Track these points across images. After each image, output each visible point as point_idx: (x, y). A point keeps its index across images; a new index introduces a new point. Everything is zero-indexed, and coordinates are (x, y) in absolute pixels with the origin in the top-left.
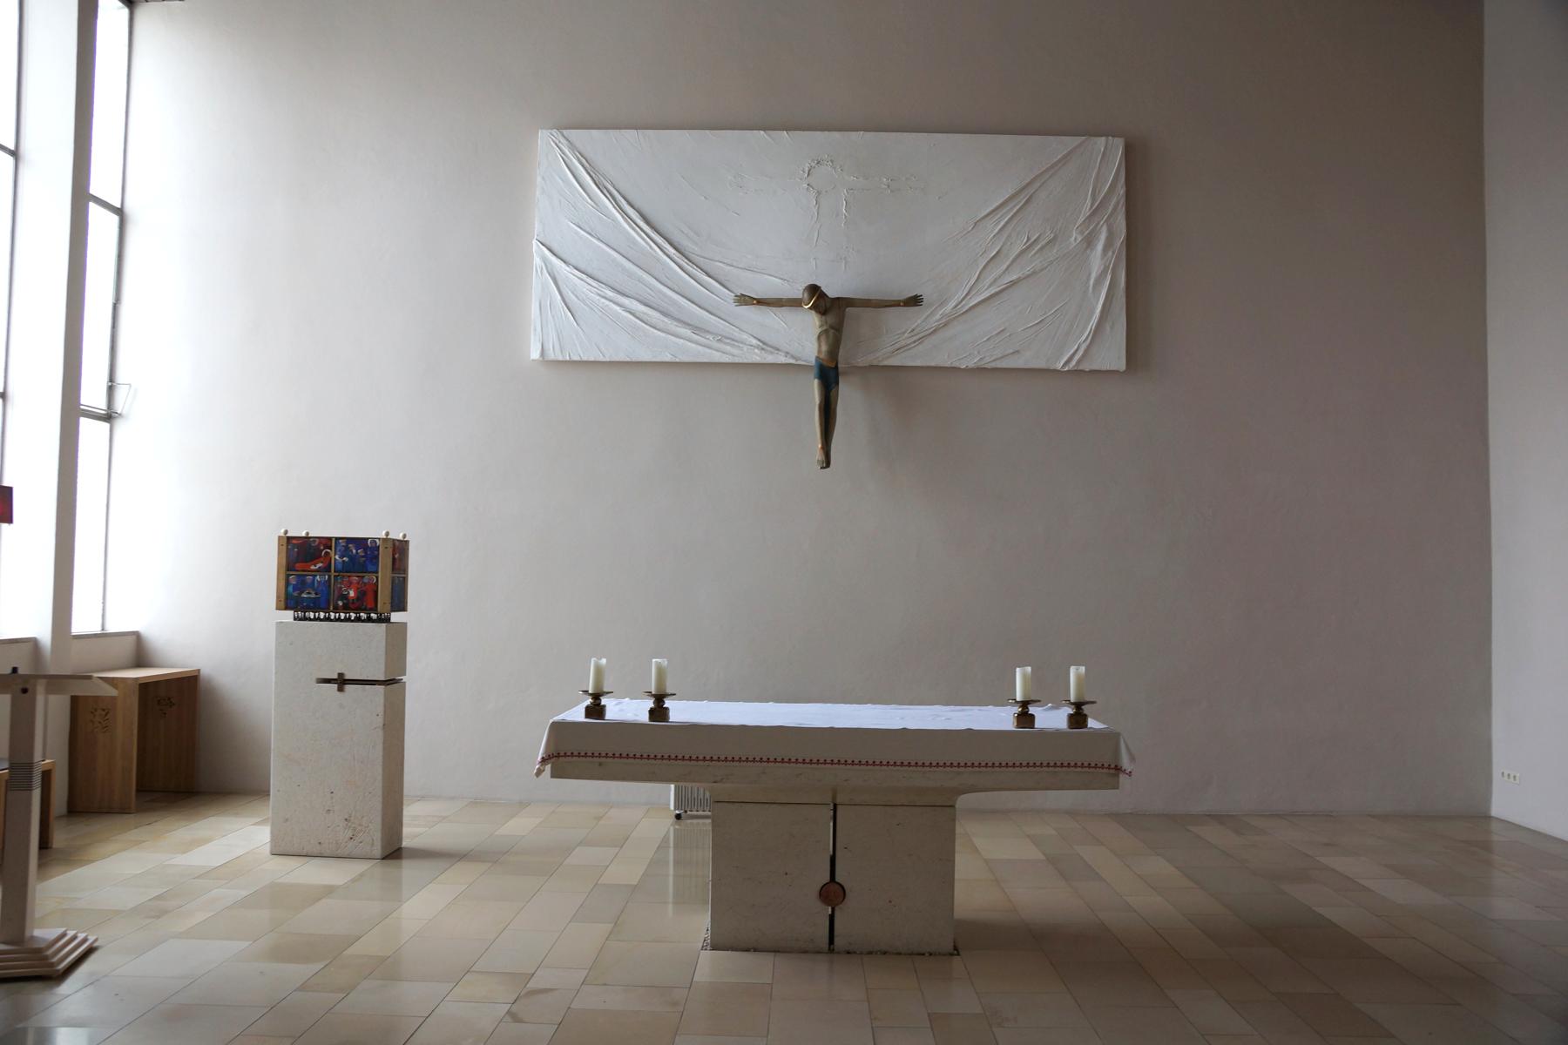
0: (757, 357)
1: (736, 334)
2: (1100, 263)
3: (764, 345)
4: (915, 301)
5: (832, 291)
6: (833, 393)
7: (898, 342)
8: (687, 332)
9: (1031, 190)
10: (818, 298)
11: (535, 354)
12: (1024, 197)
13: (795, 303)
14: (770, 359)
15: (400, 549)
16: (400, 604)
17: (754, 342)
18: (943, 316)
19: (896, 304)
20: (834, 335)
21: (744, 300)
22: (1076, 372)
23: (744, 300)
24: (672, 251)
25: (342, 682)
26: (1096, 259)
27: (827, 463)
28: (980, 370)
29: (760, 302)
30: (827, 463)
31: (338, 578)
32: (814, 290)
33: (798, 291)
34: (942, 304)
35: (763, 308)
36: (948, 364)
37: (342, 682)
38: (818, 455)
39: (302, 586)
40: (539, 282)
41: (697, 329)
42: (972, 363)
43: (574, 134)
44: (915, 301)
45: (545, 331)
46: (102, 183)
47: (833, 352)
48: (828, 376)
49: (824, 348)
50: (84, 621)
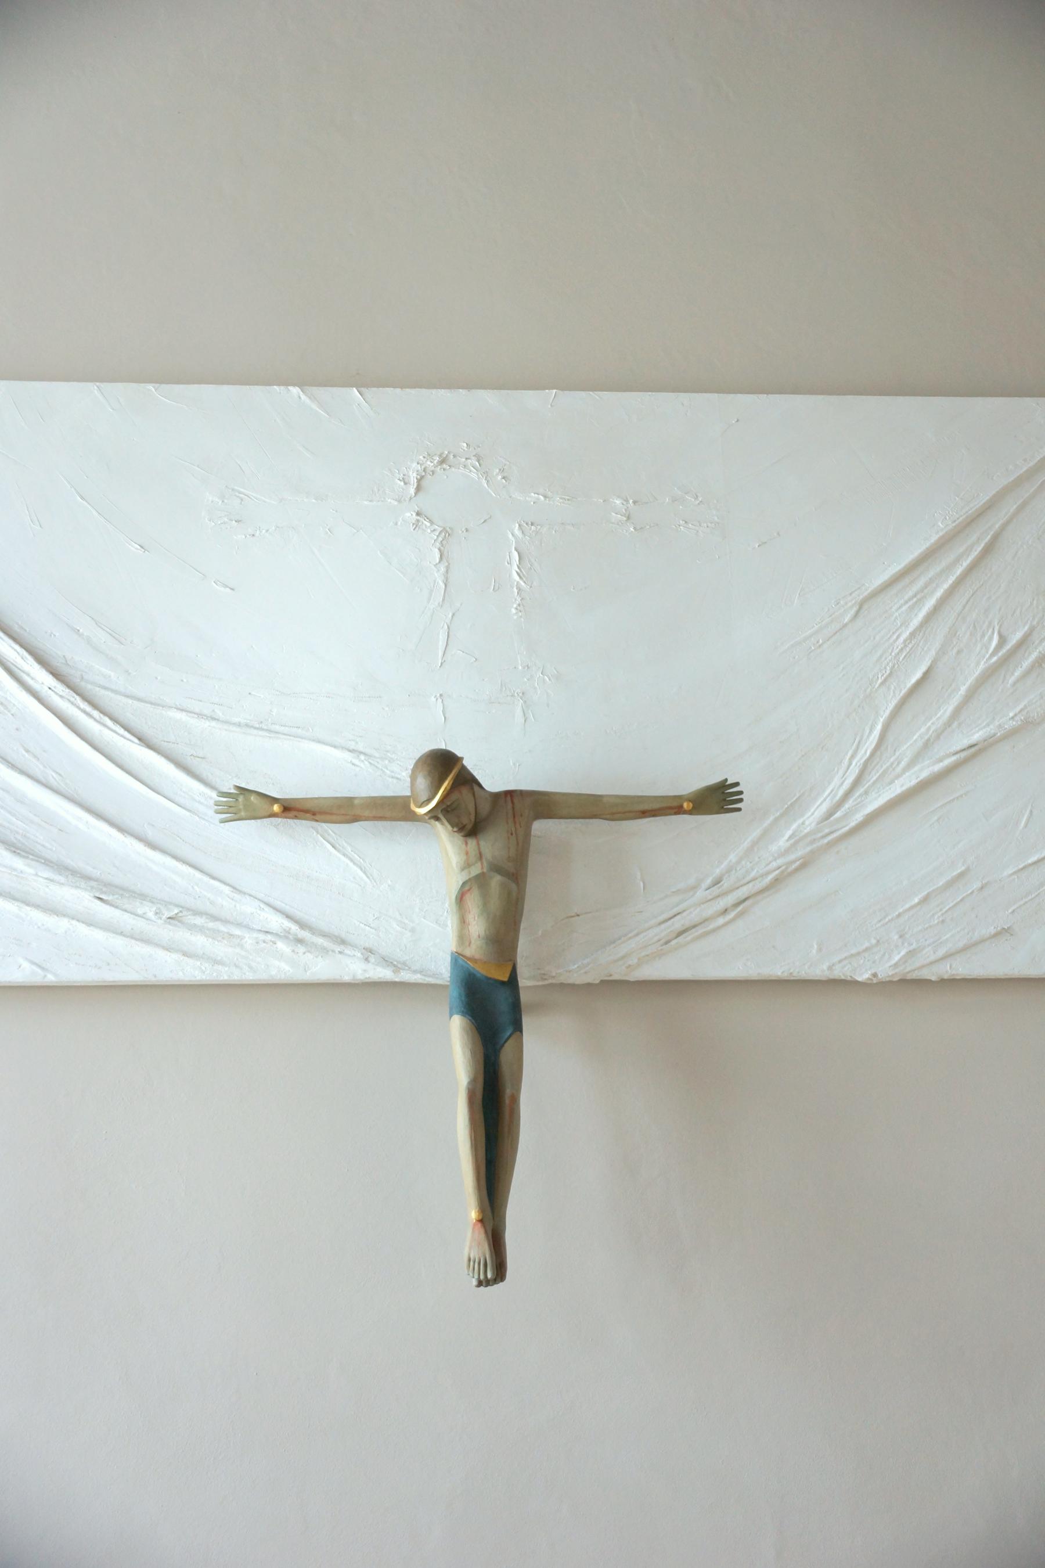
0: (282, 965)
1: (224, 900)
3: (304, 931)
4: (719, 798)
6: (506, 1054)
8: (80, 898)
9: (996, 520)
10: (454, 790)
12: (978, 539)
13: (390, 810)
14: (321, 968)
17: (277, 922)
18: (796, 841)
20: (505, 892)
21: (246, 804)
23: (246, 804)
24: (41, 679)
27: (496, 1268)
29: (291, 809)
30: (496, 1268)
32: (443, 764)
33: (397, 776)
34: (792, 809)
35: (301, 827)
36: (820, 971)
38: (468, 1241)
41: (107, 890)
42: (885, 970)
44: (719, 798)
47: (504, 937)
48: (491, 1007)
49: (477, 927)
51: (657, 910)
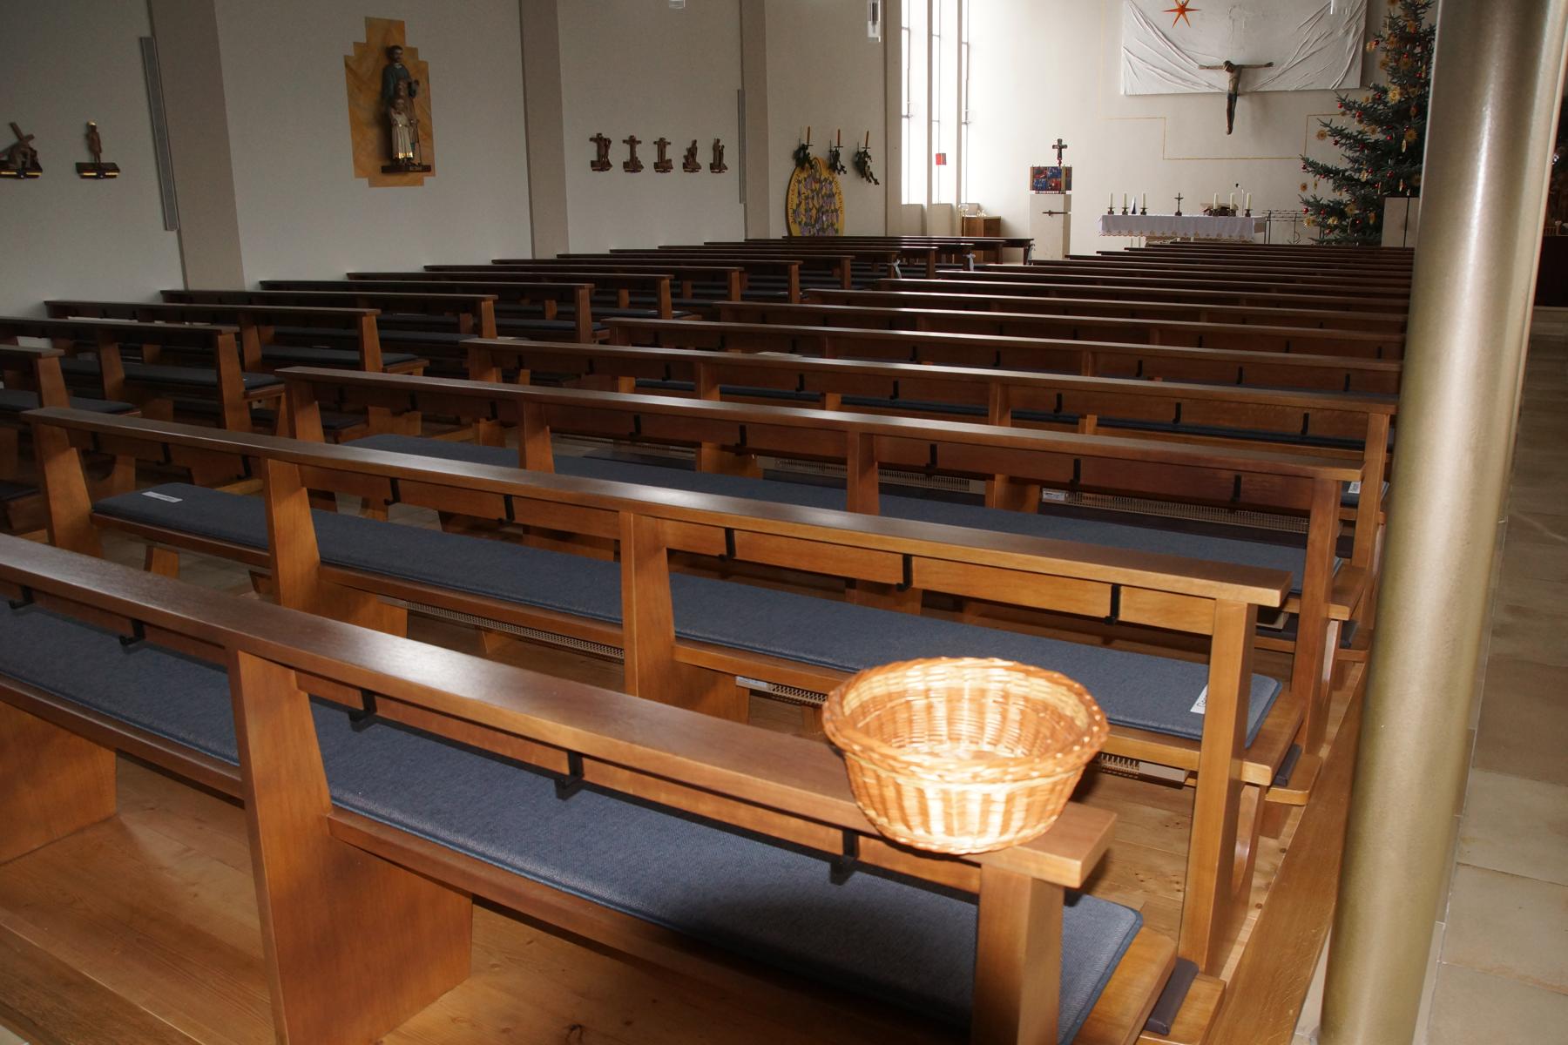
3: (1210, 85)
4: (1270, 65)
5: (1235, 62)
10: (1229, 66)
16: (1069, 187)
20: (1236, 81)
21: (1202, 67)
23: (1202, 67)
25: (1050, 213)
26: (1350, 40)
27: (1230, 131)
30: (1230, 131)
31: (1051, 180)
32: (1228, 63)
33: (1222, 63)
37: (1050, 213)
38: (1226, 128)
40: (1124, 64)
44: (1270, 65)
45: (1127, 81)
46: (964, 39)
48: (1232, 99)
50: (935, 201)
51: (1265, 81)
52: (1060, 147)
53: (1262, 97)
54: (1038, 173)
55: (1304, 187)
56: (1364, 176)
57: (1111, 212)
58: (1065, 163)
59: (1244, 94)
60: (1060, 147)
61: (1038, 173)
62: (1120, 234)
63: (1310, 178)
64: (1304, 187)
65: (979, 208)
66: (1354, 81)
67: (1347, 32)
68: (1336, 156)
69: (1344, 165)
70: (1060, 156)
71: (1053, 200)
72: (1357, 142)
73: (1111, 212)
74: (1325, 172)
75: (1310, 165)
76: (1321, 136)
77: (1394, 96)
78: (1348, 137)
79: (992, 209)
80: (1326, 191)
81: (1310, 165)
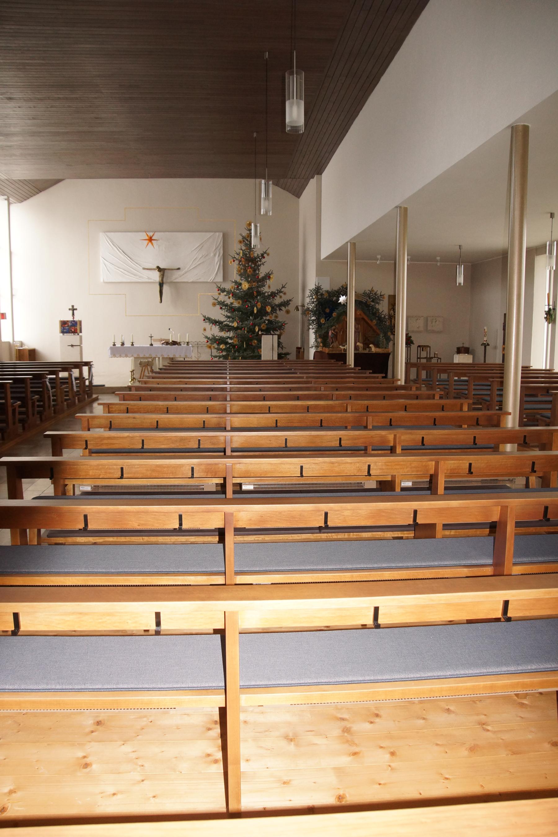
0: (147, 280)
2: (217, 261)
3: (149, 278)
5: (162, 267)
7: (177, 277)
10: (159, 269)
11: (102, 281)
12: (201, 246)
13: (154, 269)
14: (150, 281)
15: (80, 322)
16: (81, 332)
19: (175, 269)
20: (163, 276)
21: (144, 269)
22: (212, 282)
23: (144, 269)
25: (72, 346)
26: (216, 259)
27: (161, 302)
28: (192, 282)
29: (147, 269)
31: (70, 327)
32: (158, 267)
33: (155, 267)
37: (72, 346)
39: (64, 329)
41: (135, 275)
42: (191, 281)
43: (108, 234)
44: (179, 269)
47: (162, 280)
48: (161, 285)
52: (73, 309)
53: (175, 285)
54: (64, 324)
55: (205, 330)
56: (235, 324)
57: (114, 345)
58: (76, 319)
59: (167, 283)
60: (73, 309)
61: (64, 324)
62: (120, 356)
63: (208, 325)
64: (205, 330)
65: (22, 344)
66: (220, 279)
67: (215, 255)
68: (219, 314)
69: (223, 319)
70: (73, 314)
71: (71, 338)
72: (231, 309)
73: (114, 345)
74: (215, 322)
75: (207, 319)
76: (214, 305)
77: (245, 286)
78: (226, 305)
79: (30, 343)
80: (215, 331)
81: (207, 319)
